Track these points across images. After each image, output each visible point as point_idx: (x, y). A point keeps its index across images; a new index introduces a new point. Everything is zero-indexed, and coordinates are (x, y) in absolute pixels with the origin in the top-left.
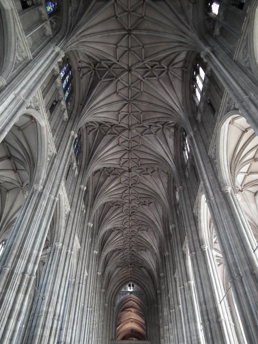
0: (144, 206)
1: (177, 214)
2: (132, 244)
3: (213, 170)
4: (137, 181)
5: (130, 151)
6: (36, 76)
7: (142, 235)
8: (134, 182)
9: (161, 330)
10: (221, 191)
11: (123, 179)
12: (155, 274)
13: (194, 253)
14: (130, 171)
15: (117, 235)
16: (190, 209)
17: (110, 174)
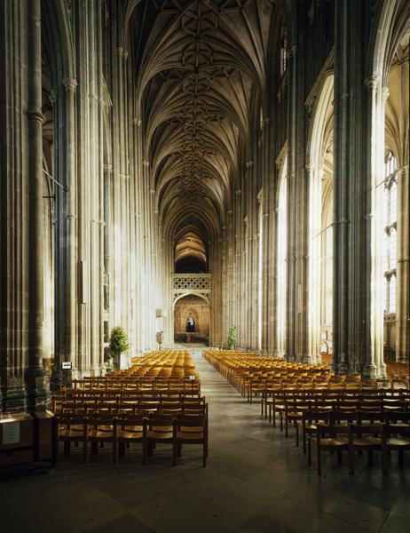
0: (214, 123)
1: (257, 145)
2: (195, 170)
3: (305, 133)
4: (206, 87)
5: (198, 38)
6: (93, 34)
7: (209, 161)
8: (201, 87)
9: (224, 267)
10: (304, 168)
11: (186, 83)
12: (222, 207)
13: (267, 215)
14: (197, 71)
15: (174, 161)
16: (272, 157)
17: (166, 76)
